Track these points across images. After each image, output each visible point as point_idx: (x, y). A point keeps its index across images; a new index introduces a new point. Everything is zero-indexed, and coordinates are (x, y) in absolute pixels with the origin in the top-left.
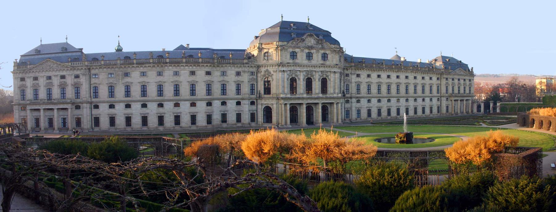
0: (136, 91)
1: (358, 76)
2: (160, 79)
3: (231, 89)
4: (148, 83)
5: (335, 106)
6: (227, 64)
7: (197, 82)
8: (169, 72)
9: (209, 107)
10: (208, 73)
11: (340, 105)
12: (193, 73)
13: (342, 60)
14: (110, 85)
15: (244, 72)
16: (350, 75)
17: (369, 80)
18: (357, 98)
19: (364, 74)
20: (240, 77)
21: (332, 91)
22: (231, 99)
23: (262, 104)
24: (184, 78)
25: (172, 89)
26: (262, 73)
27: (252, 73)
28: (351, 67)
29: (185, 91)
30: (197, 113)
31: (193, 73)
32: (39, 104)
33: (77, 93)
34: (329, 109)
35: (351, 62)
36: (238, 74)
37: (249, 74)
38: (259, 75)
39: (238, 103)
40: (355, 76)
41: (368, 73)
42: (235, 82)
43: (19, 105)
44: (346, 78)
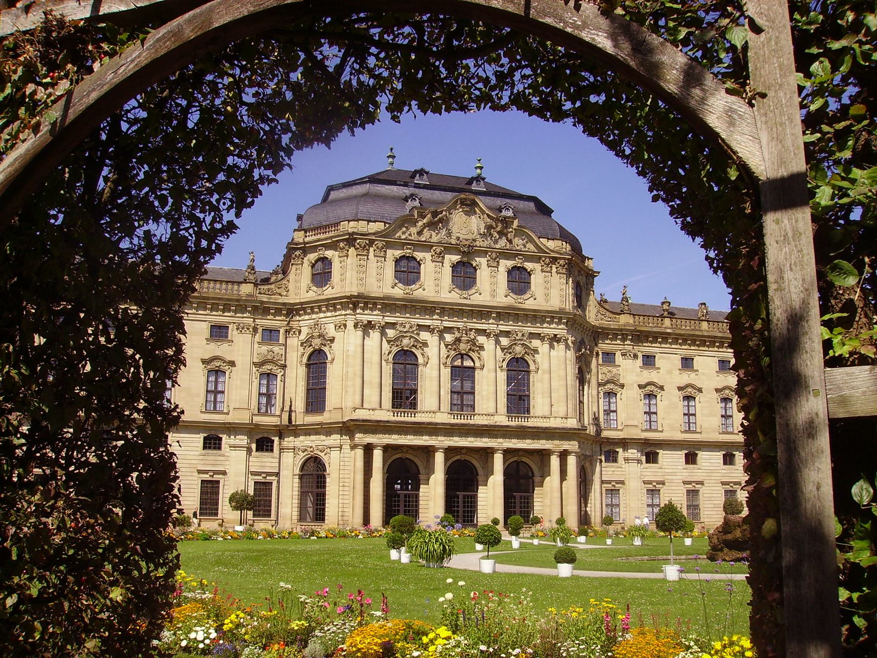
1: (649, 361)
5: (555, 461)
11: (572, 461)
15: (240, 328)
16: (618, 358)
17: (686, 378)
20: (225, 345)
26: (303, 337)
34: (537, 479)
35: (622, 312)
36: (219, 332)
37: (258, 338)
42: (204, 362)
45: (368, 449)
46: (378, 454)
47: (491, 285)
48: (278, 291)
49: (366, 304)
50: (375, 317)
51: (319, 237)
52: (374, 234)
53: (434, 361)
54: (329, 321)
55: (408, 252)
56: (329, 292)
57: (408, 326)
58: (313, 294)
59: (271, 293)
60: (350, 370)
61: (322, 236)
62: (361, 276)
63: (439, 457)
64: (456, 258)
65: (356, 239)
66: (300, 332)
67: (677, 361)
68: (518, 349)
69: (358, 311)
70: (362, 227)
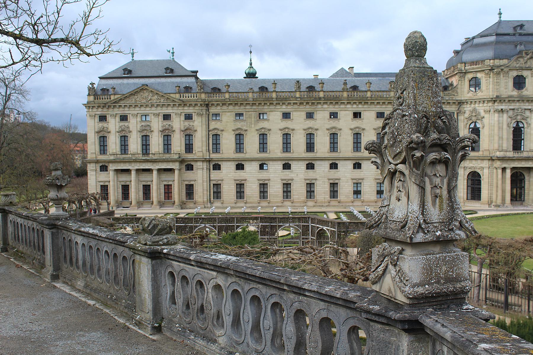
0: (275, 143)
2: (310, 123)
4: (293, 130)
7: (364, 129)
8: (322, 115)
14: (237, 132)
25: (327, 140)
26: (467, 115)
30: (363, 179)
31: (357, 115)
32: (130, 162)
33: (189, 148)
43: (97, 162)
45: (504, 169)
48: (453, 94)
49: (500, 100)
50: (504, 107)
51: (473, 67)
52: (502, 66)
54: (481, 108)
55: (520, 73)
56: (480, 94)
57: (520, 110)
58: (470, 95)
59: (448, 95)
60: (492, 132)
61: (474, 66)
62: (497, 87)
65: (494, 69)
66: (465, 113)
69: (496, 104)
70: (497, 62)
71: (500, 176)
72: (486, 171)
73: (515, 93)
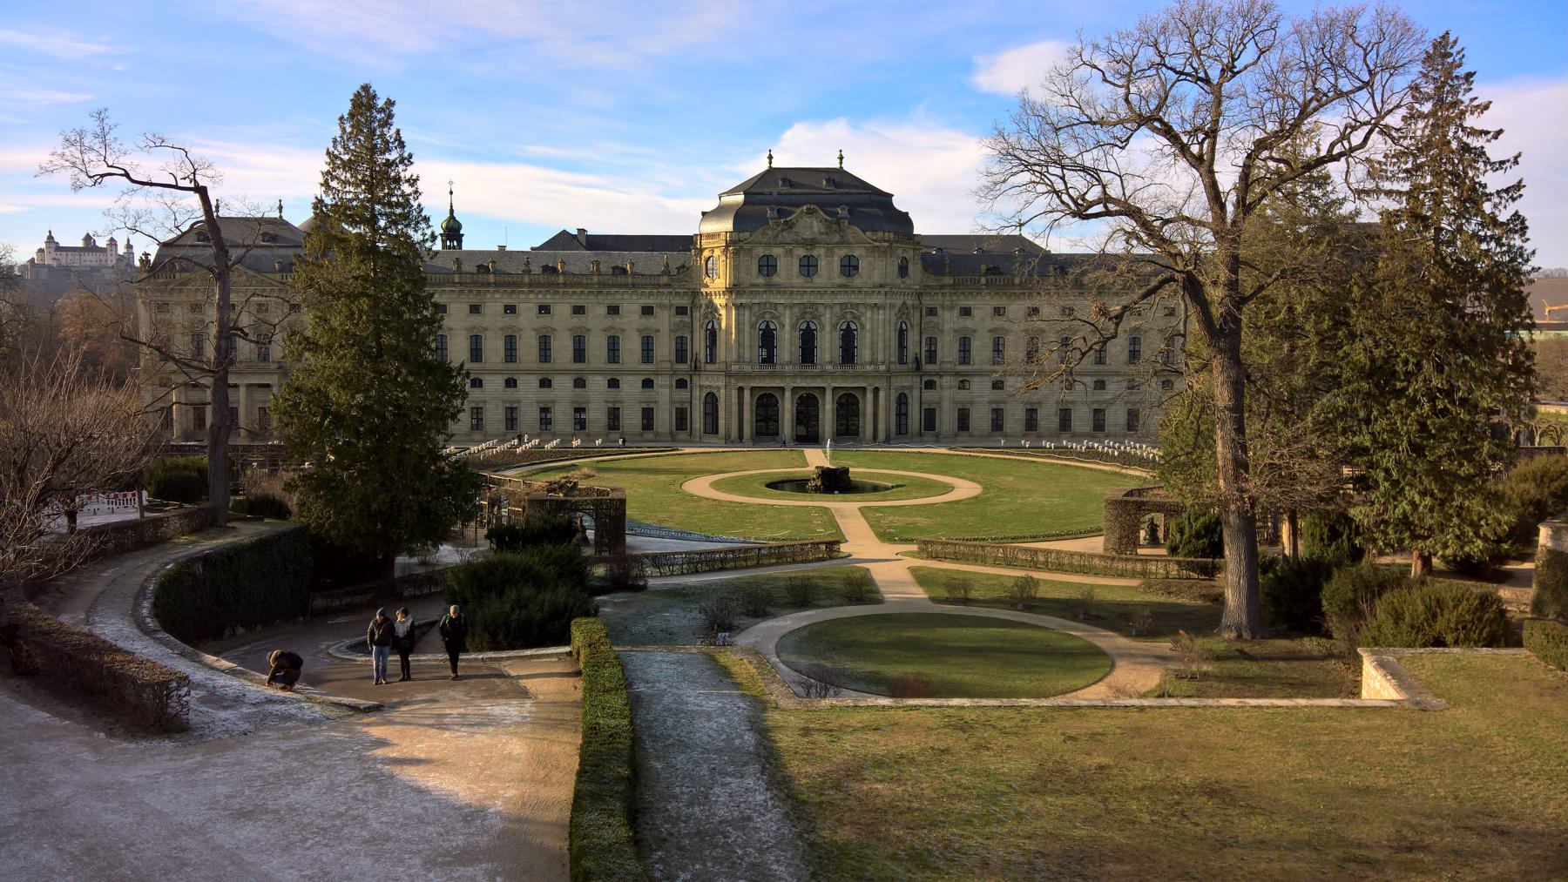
1: (966, 312)
2: (475, 320)
3: (631, 348)
5: (870, 396)
6: (622, 286)
9: (579, 391)
10: (579, 310)
11: (882, 394)
12: (544, 309)
13: (915, 269)
15: (661, 306)
16: (940, 311)
18: (957, 374)
19: (982, 306)
21: (868, 358)
22: (631, 372)
23: (701, 387)
24: (527, 321)
27: (681, 311)
28: (942, 287)
29: (528, 349)
31: (544, 309)
35: (944, 274)
36: (647, 311)
37: (673, 311)
38: (697, 314)
39: (648, 384)
40: (956, 312)
41: (996, 302)
44: (926, 319)
45: (741, 389)
46: (747, 393)
47: (829, 268)
53: (787, 328)
63: (788, 394)
64: (801, 252)
67: (989, 310)
68: (849, 317)
71: (735, 399)
72: (722, 392)
73: (761, 280)
